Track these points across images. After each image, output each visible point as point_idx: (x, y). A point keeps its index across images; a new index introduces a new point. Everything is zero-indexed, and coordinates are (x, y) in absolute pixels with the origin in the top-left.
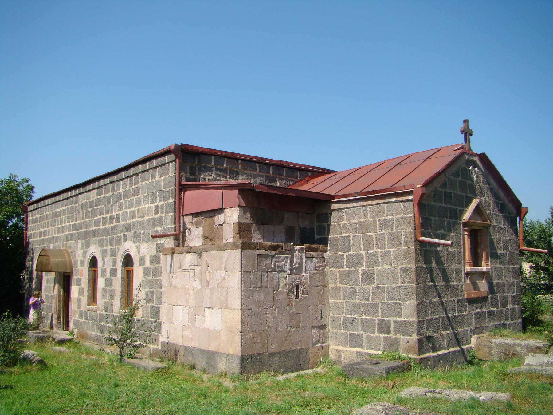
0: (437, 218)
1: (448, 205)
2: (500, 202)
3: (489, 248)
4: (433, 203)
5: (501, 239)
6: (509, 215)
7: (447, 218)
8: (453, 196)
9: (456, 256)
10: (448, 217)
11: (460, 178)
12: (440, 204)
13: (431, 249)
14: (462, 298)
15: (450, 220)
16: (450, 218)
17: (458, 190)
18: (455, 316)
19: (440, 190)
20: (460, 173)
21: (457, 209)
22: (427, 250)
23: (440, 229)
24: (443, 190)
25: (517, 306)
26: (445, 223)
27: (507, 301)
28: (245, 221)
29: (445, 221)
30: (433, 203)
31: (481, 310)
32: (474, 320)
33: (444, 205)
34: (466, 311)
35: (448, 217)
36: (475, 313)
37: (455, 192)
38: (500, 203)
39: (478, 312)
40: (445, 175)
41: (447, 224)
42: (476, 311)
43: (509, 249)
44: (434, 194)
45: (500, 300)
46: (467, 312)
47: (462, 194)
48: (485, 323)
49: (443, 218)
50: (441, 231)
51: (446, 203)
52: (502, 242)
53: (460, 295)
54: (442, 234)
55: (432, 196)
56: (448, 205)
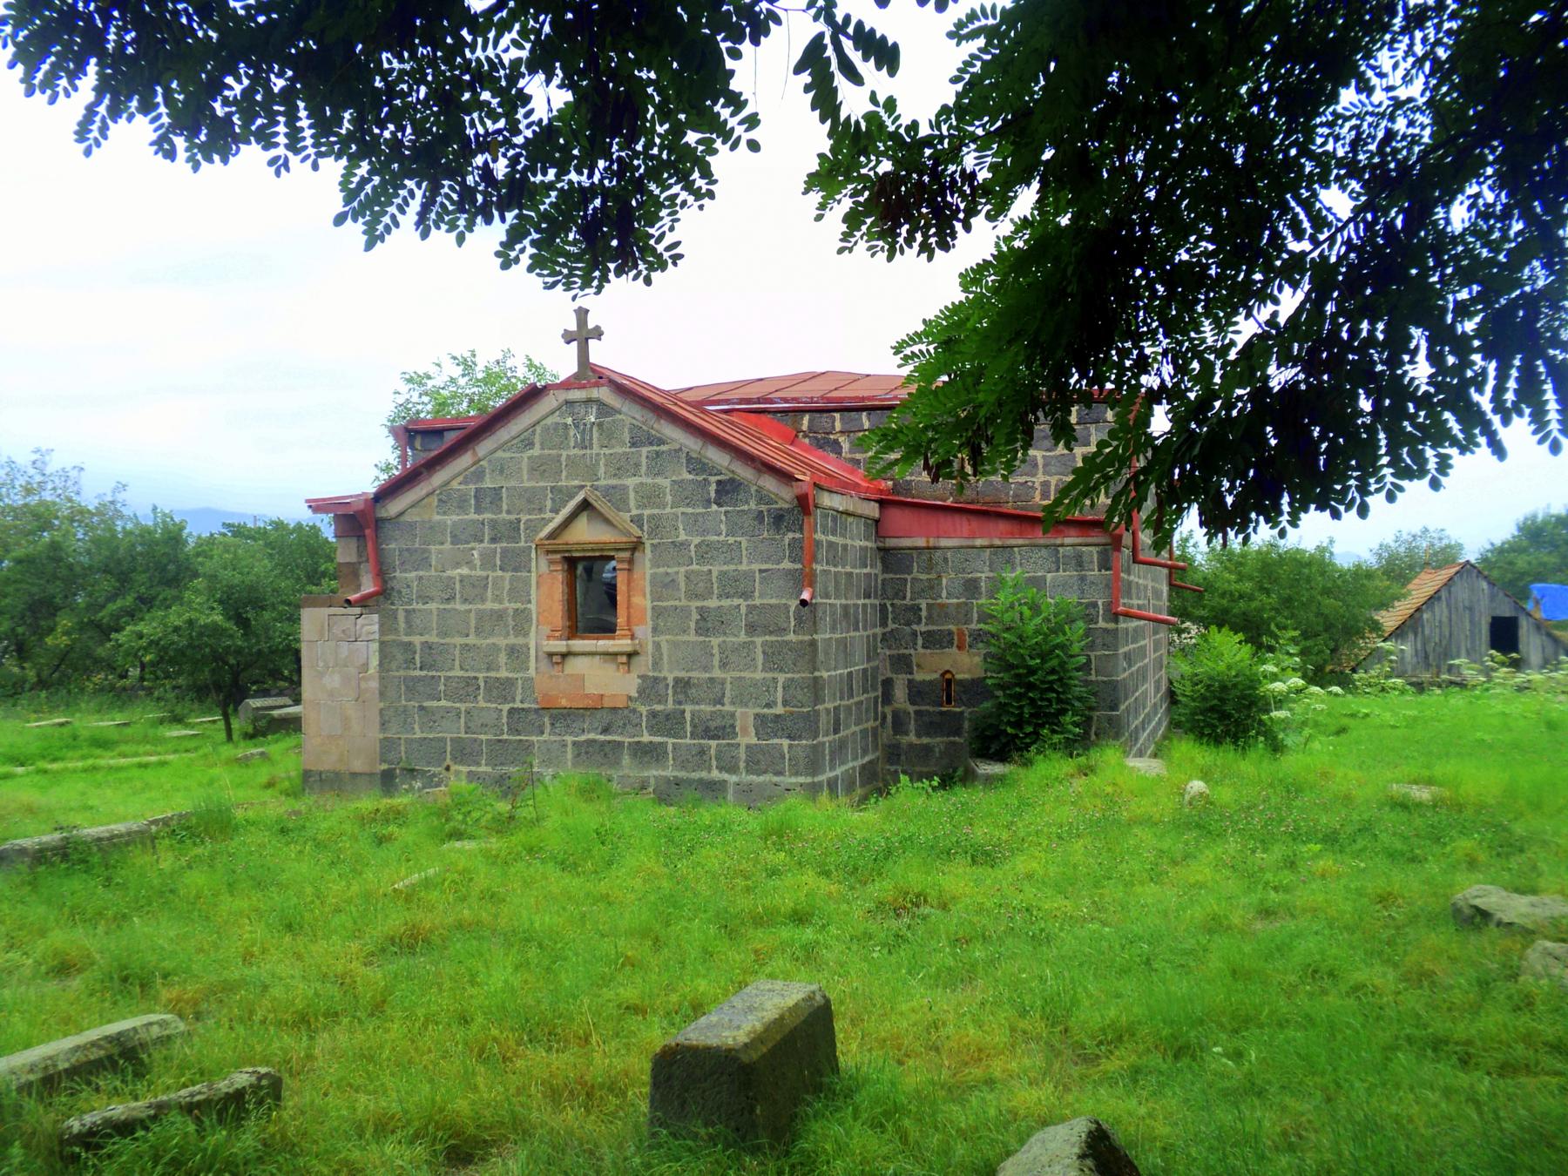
0: (448, 546)
1: (488, 516)
2: (713, 479)
3: (648, 596)
4: (437, 518)
5: (710, 571)
6: (763, 508)
7: (482, 541)
8: (504, 496)
9: (510, 619)
10: (487, 538)
11: (536, 451)
12: (455, 518)
13: (426, 607)
14: (526, 706)
15: (493, 546)
16: (493, 540)
17: (525, 477)
18: (500, 741)
19: (462, 487)
20: (537, 439)
21: (519, 521)
22: (414, 610)
23: (457, 565)
24: (472, 487)
25: (786, 742)
26: (475, 552)
27: (733, 726)
28: (348, 560)
29: (473, 549)
30: (437, 518)
31: (602, 738)
32: (569, 756)
33: (473, 516)
34: (542, 733)
35: (487, 538)
36: (574, 743)
37: (513, 483)
38: (719, 483)
39: (591, 742)
40: (475, 454)
41: (481, 555)
42: (582, 738)
43: (757, 594)
44: (440, 500)
45: (692, 719)
46: (545, 737)
47: (542, 484)
48: (617, 763)
49: (468, 543)
50: (459, 571)
51: (478, 510)
52: (714, 580)
53: (518, 698)
54: (461, 575)
55: (436, 503)
56: (488, 516)
